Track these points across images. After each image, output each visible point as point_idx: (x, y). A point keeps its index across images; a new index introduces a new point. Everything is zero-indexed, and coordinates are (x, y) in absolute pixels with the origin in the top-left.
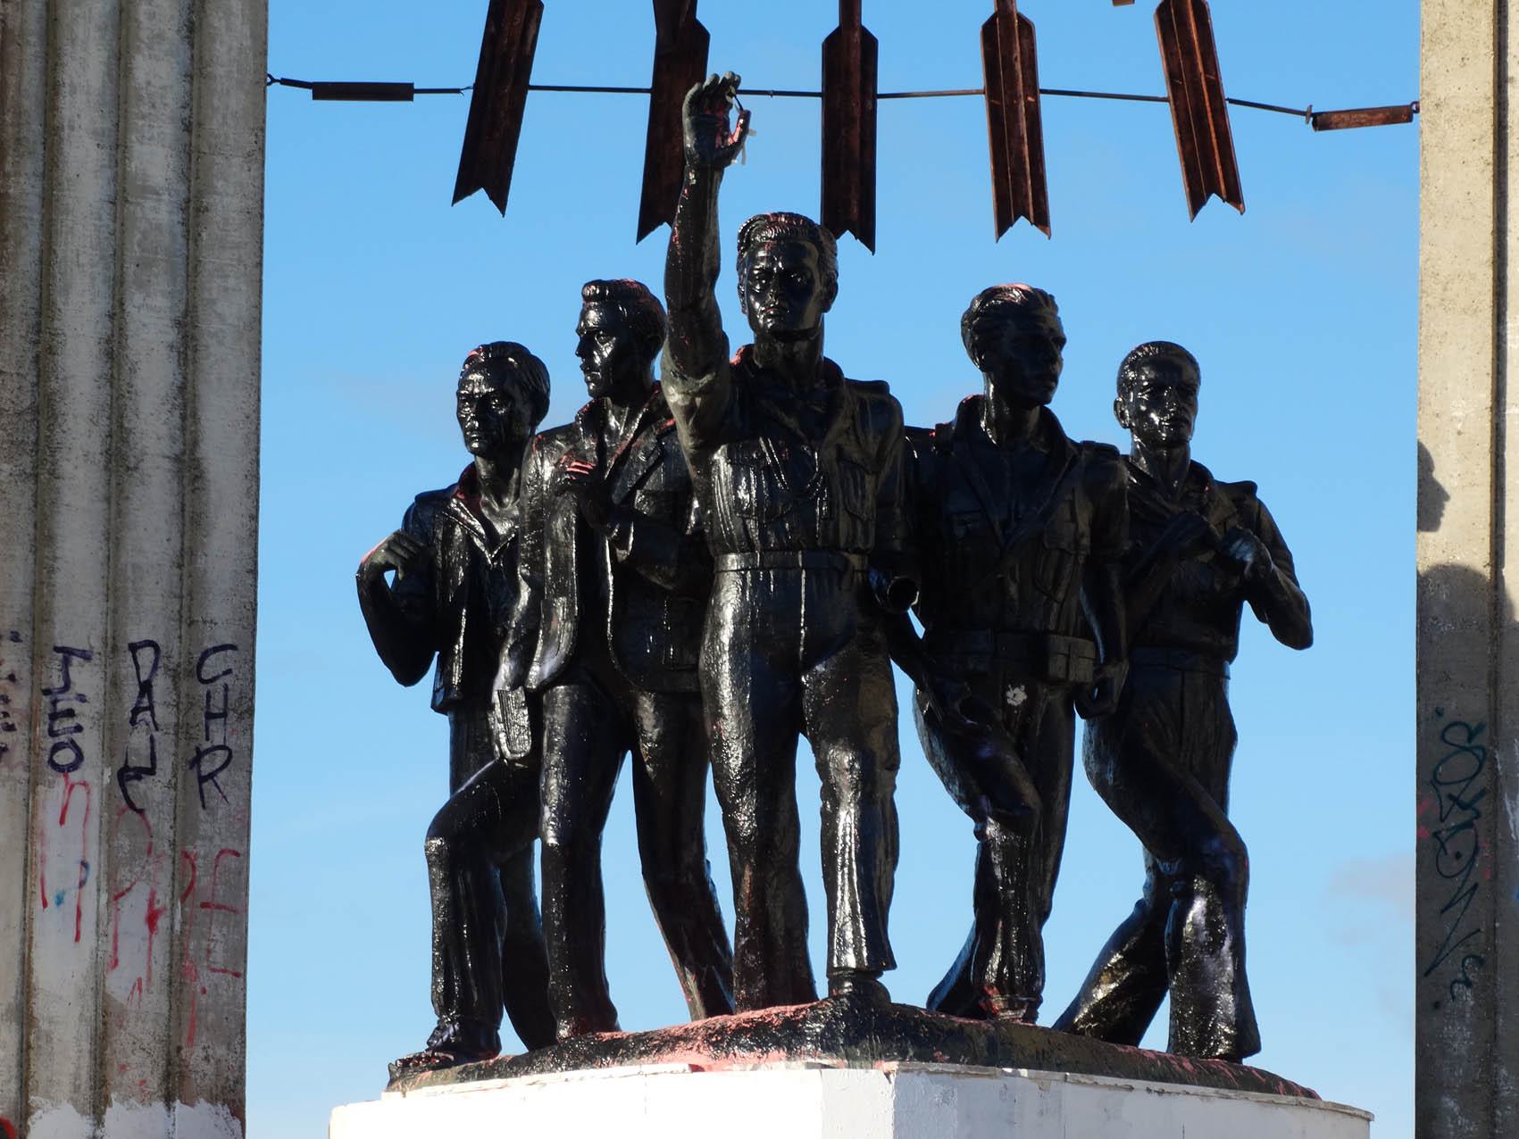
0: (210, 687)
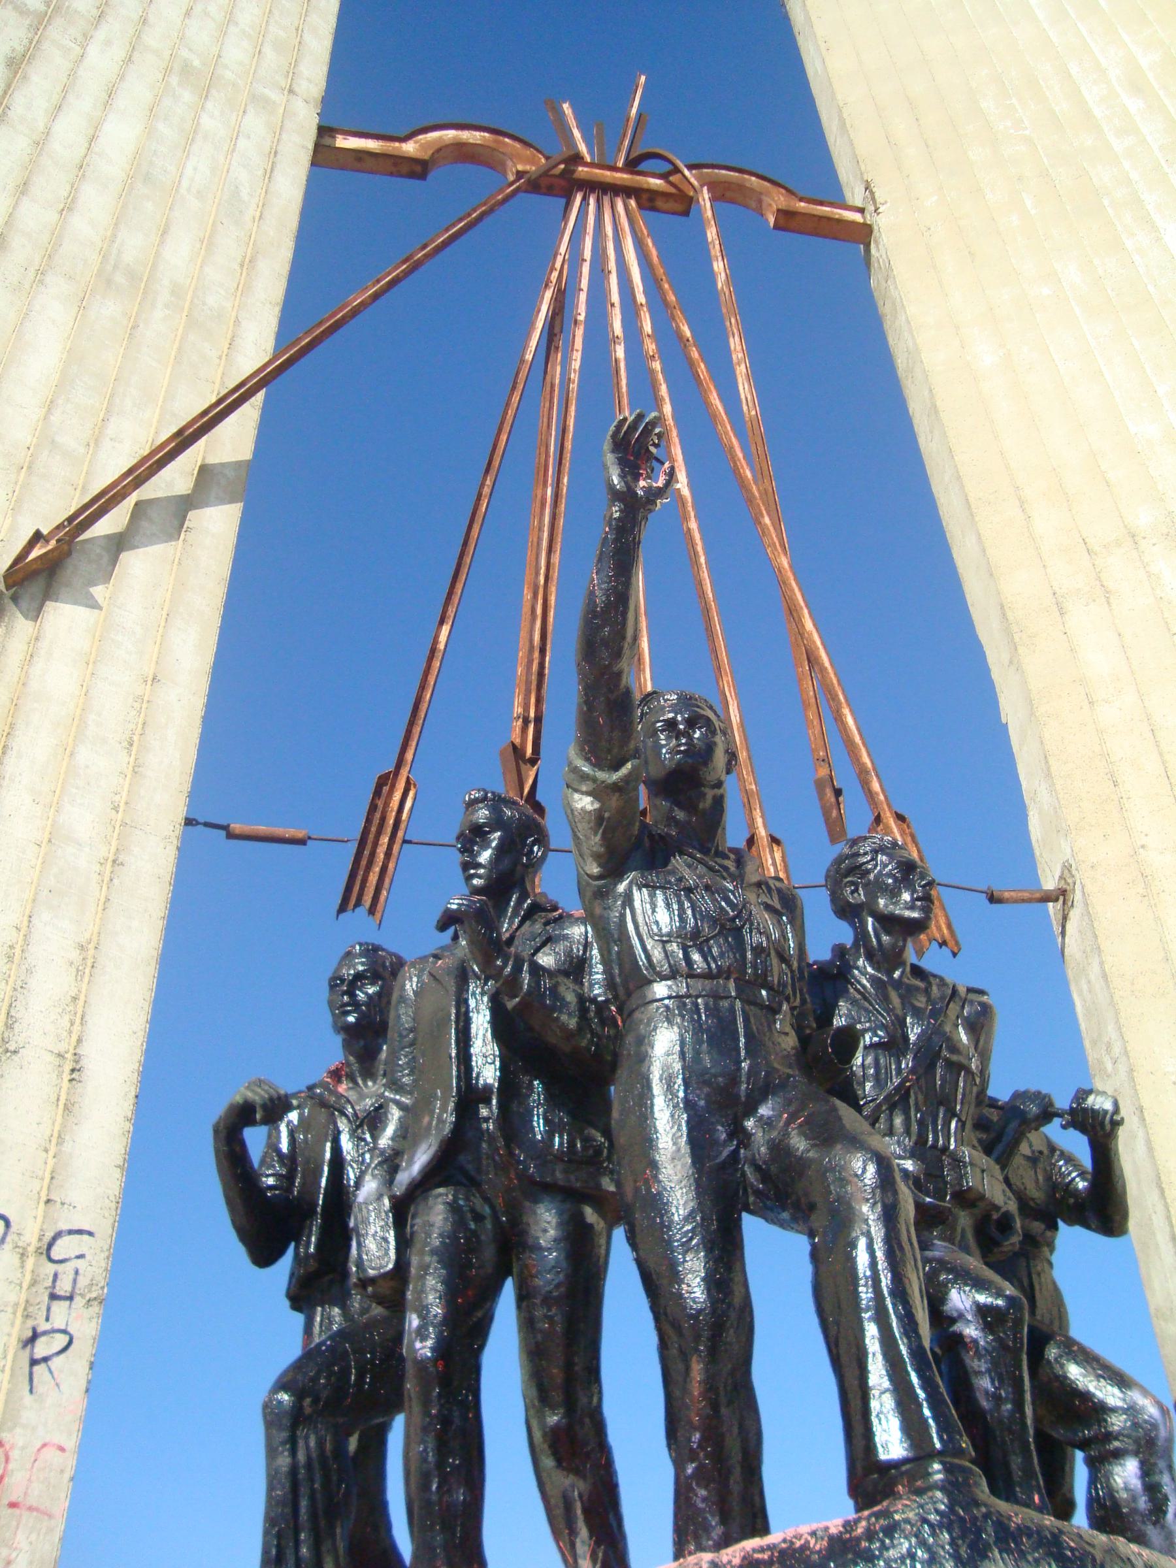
0: (60, 1268)
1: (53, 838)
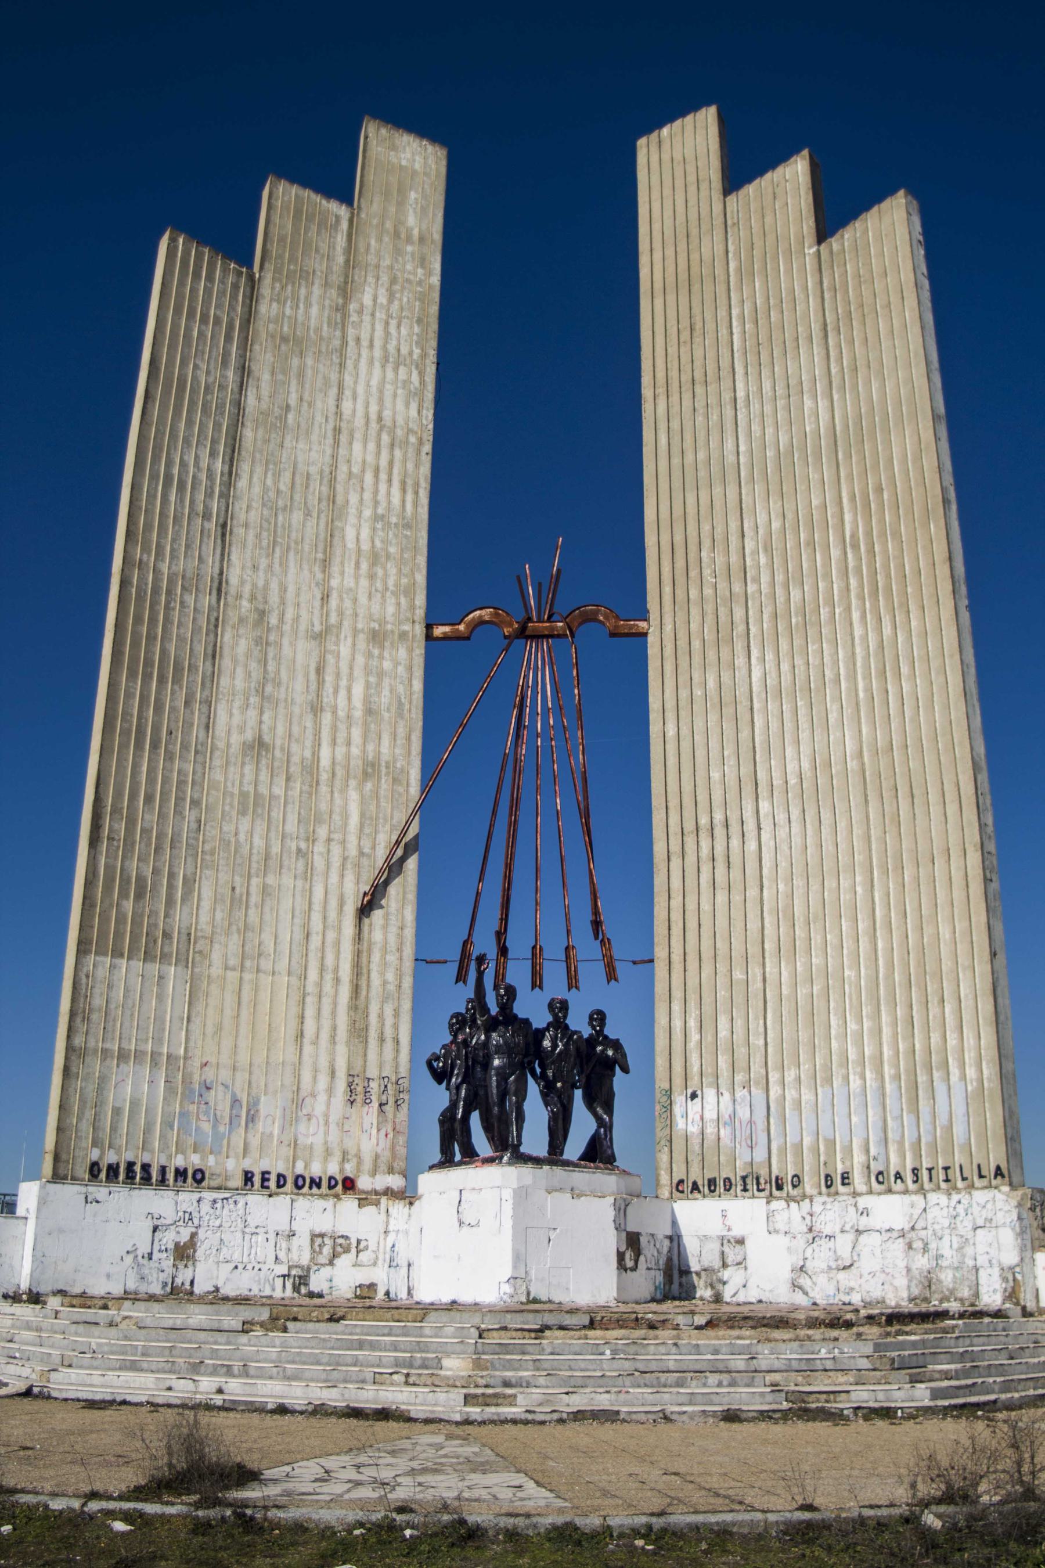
1: (385, 983)
